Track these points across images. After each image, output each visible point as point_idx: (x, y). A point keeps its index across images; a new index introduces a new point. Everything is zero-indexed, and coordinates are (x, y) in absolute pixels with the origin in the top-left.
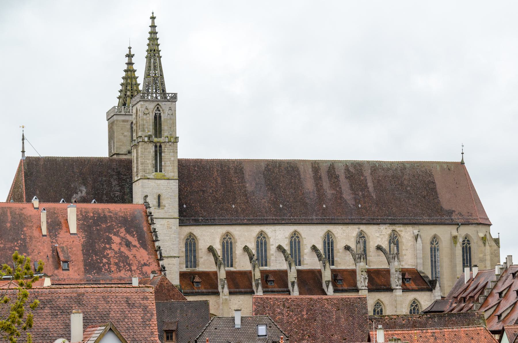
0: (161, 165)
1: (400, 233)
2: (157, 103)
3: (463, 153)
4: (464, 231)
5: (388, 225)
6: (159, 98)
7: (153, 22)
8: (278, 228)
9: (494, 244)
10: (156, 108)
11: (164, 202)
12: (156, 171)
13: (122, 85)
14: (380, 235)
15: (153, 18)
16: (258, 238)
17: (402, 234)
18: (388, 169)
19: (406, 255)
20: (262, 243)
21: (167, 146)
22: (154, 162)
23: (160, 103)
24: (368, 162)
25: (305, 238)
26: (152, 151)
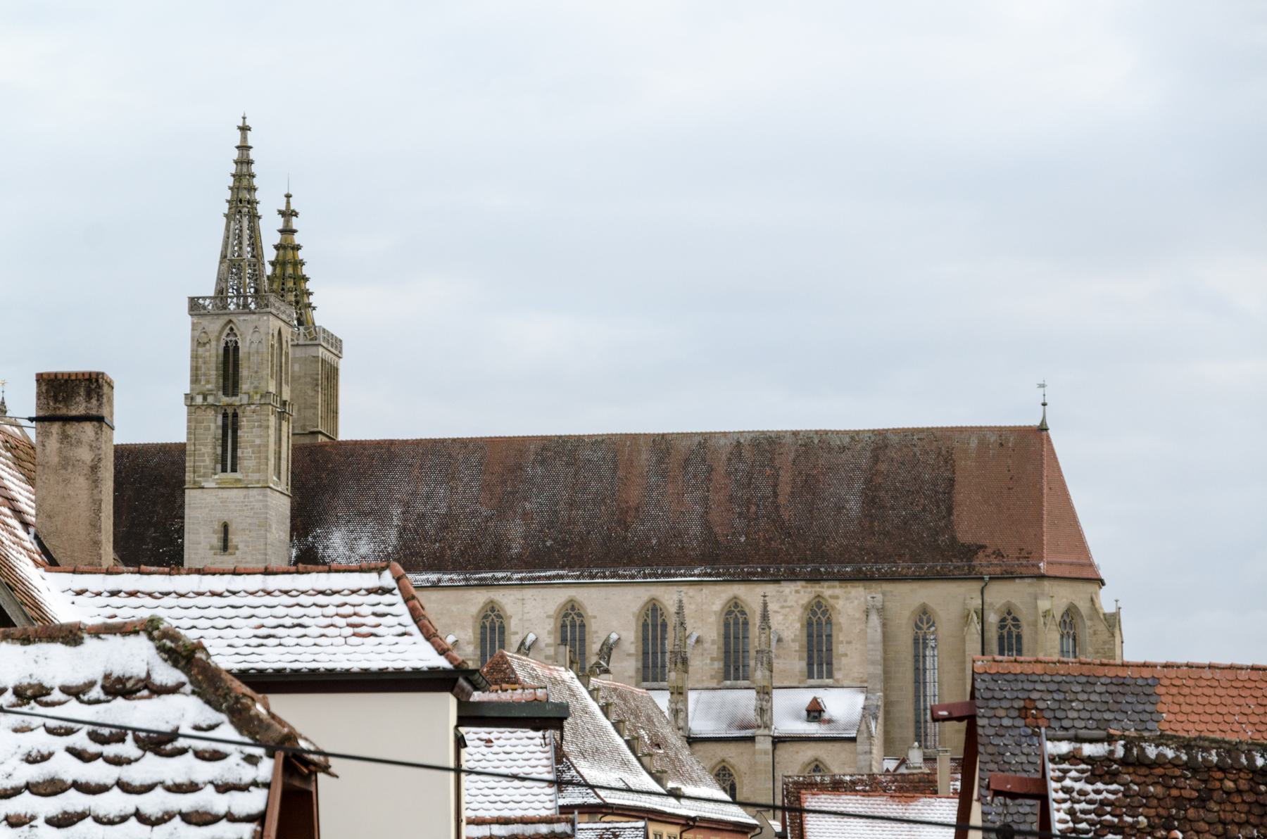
0: (234, 457)
1: (832, 601)
2: (226, 318)
3: (1044, 404)
4: (1001, 595)
5: (803, 583)
6: (253, 306)
7: (244, 138)
8: (529, 593)
9: (1102, 627)
10: (227, 330)
11: (234, 539)
12: (224, 470)
13: (305, 279)
14: (782, 607)
15: (244, 129)
16: (486, 617)
17: (840, 604)
18: (843, 449)
19: (846, 655)
20: (492, 629)
21: (247, 413)
22: (219, 450)
23: (234, 319)
24: (795, 434)
25: (595, 617)
26: (213, 426)
